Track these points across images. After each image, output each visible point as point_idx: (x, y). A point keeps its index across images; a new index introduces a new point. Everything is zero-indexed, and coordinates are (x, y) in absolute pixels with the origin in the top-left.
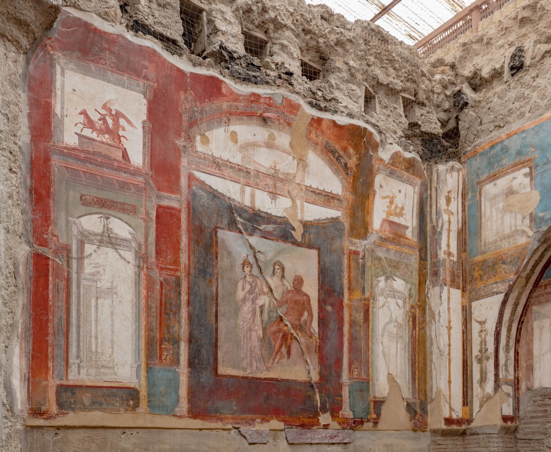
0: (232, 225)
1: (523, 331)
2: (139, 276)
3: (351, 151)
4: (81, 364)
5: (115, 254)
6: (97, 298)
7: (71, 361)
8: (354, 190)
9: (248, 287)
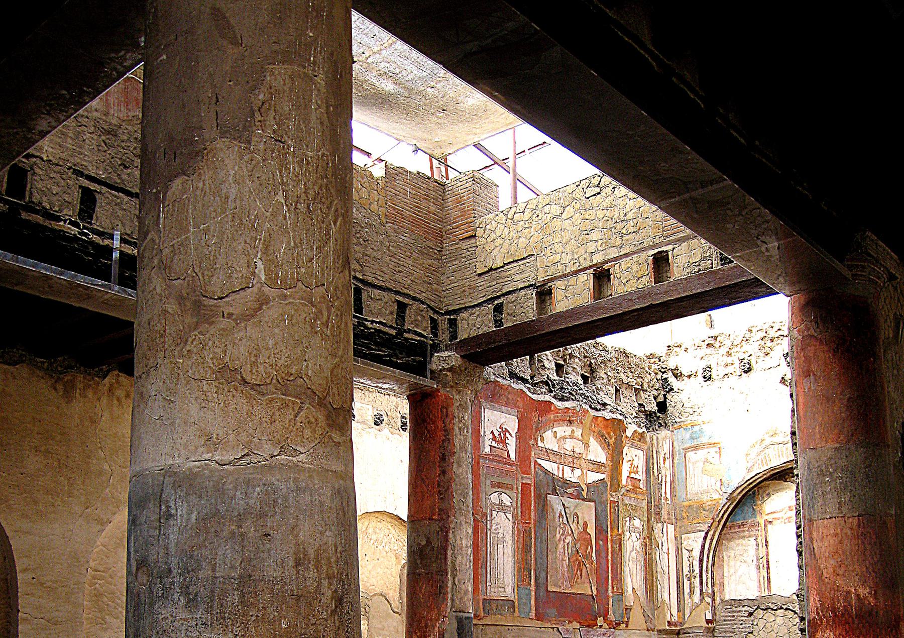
0: (554, 492)
3: (612, 434)
8: (612, 461)
9: (561, 531)
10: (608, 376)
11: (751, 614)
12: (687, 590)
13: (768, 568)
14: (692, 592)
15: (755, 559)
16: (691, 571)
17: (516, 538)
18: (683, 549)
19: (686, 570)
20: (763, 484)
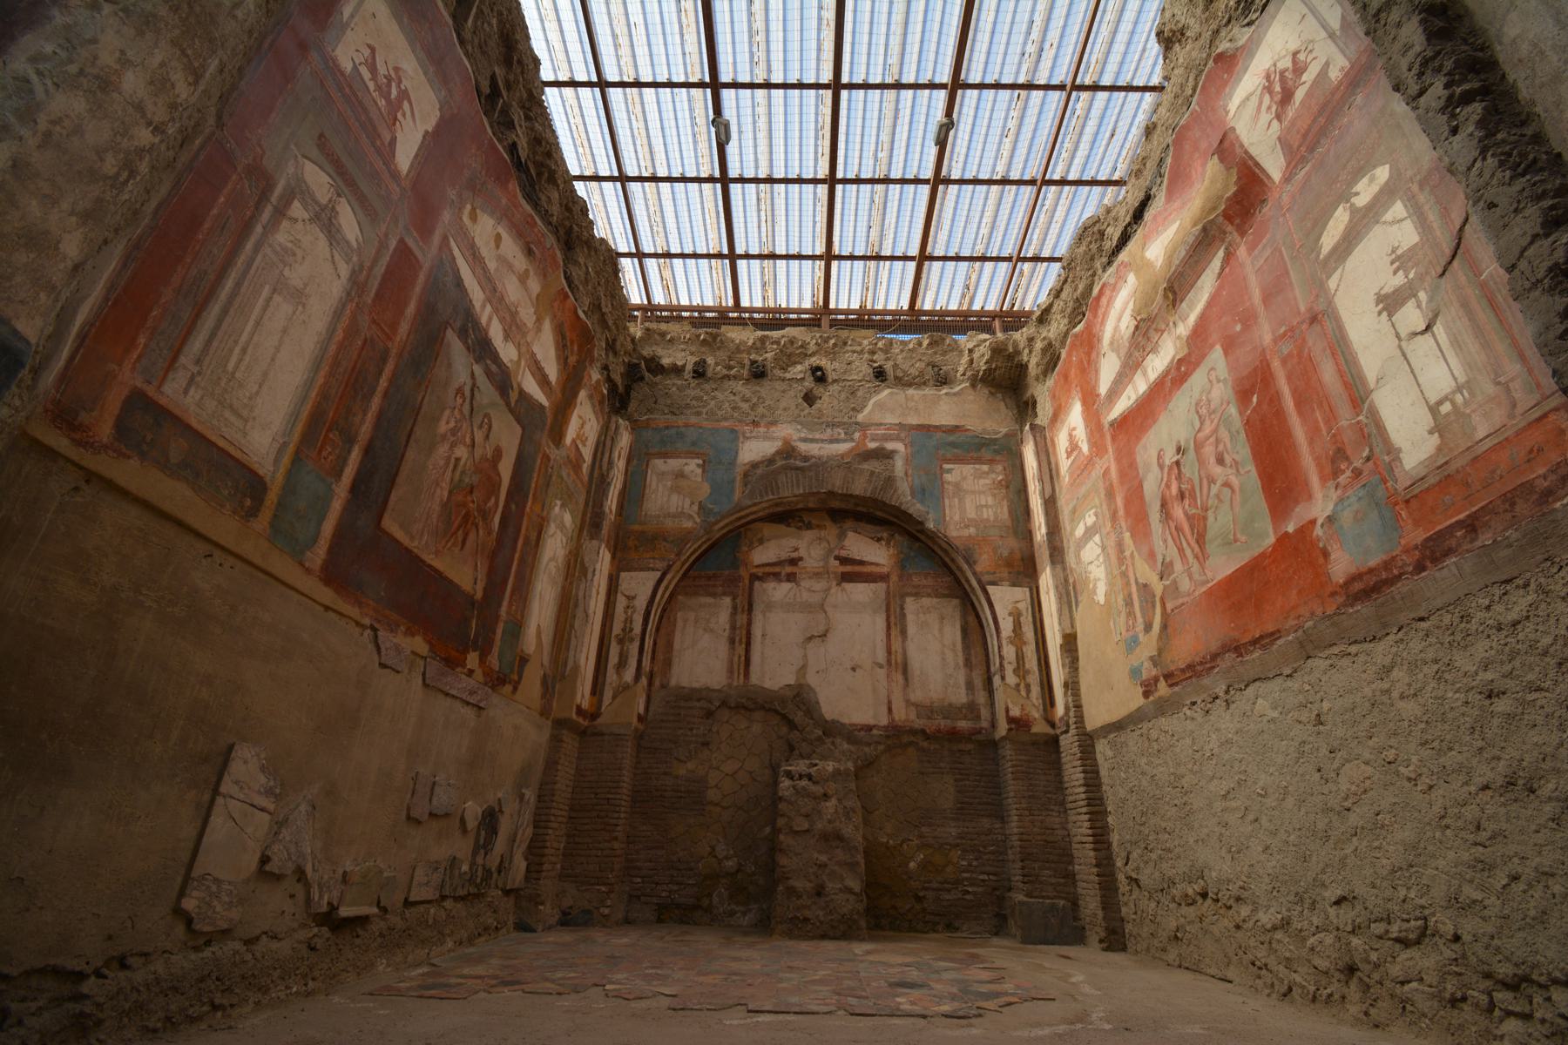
0: (463, 334)
1: (664, 620)
2: (344, 306)
3: (576, 348)
4: (198, 379)
5: (328, 249)
6: (274, 291)
7: (183, 360)
8: (564, 390)
9: (452, 424)
10: (587, 273)
11: (709, 714)
12: (613, 658)
13: (748, 644)
14: (622, 664)
15: (727, 627)
16: (627, 629)
17: (339, 335)
18: (619, 595)
19: (617, 629)
20: (752, 526)
